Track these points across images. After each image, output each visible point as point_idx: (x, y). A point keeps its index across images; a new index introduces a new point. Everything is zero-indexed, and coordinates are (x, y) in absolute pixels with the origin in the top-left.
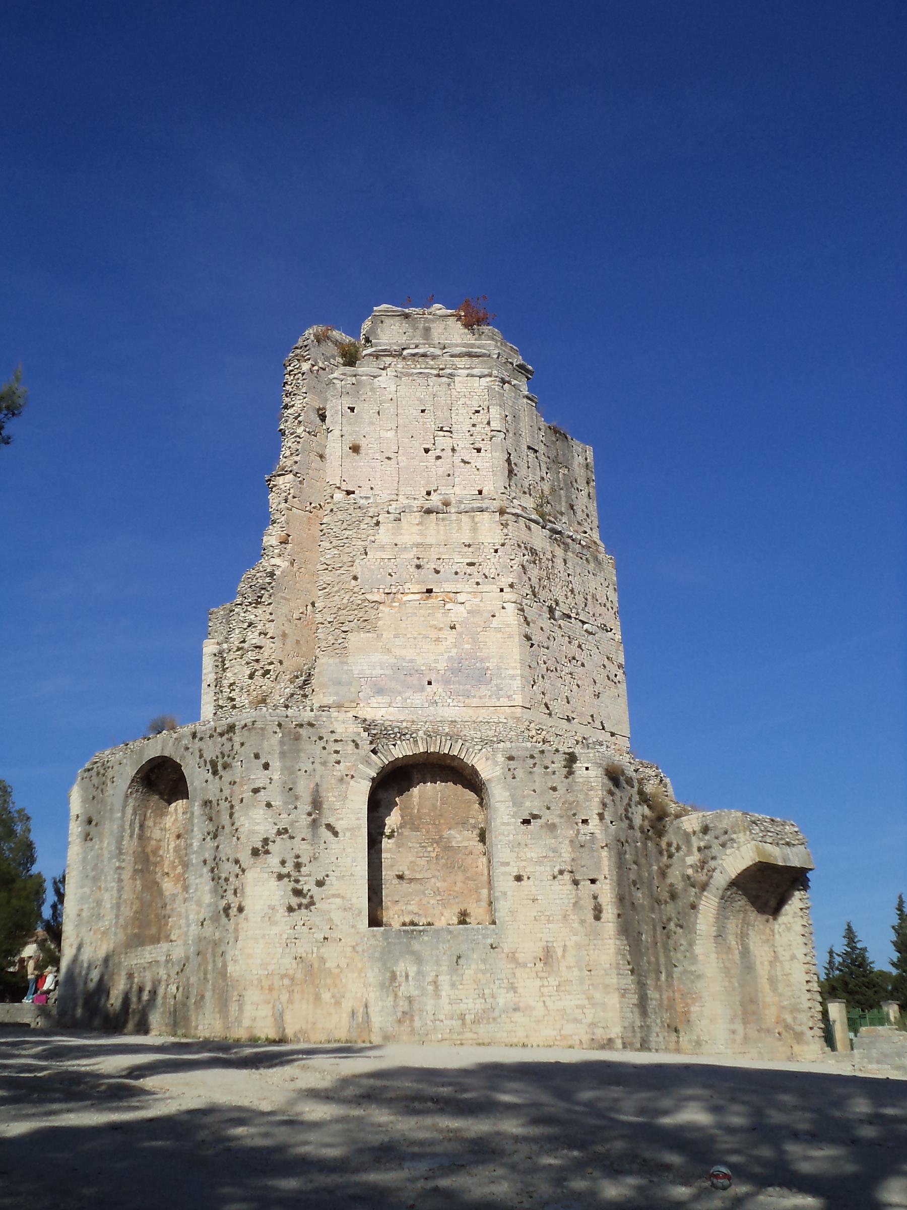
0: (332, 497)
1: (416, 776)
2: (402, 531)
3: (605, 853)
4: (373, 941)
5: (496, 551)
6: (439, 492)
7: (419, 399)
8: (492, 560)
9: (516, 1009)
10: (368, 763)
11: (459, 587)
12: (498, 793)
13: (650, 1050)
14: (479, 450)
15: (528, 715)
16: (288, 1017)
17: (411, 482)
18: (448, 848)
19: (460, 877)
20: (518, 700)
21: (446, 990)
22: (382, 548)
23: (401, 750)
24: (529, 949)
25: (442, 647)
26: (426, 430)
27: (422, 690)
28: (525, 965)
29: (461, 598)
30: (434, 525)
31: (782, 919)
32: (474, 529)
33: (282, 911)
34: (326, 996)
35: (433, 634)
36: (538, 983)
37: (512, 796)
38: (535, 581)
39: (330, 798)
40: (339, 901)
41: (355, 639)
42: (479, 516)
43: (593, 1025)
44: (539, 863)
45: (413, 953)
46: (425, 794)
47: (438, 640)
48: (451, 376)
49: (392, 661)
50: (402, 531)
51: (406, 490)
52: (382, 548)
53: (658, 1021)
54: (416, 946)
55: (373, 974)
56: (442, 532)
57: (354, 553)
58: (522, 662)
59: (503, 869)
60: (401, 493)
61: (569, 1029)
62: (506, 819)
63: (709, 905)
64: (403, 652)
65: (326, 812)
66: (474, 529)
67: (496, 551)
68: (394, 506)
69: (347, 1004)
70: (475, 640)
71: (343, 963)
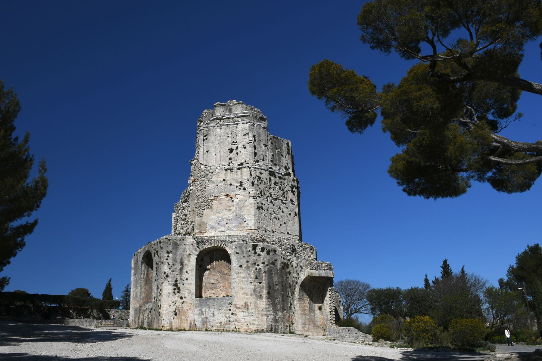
1: (215, 253)
7: (227, 133)
9: (236, 321)
10: (196, 251)
11: (236, 193)
12: (233, 258)
13: (278, 333)
14: (245, 148)
15: (256, 232)
16: (173, 324)
18: (223, 274)
19: (227, 282)
21: (216, 316)
22: (214, 182)
24: (240, 303)
25: (231, 212)
27: (225, 226)
28: (239, 308)
29: (237, 196)
32: (242, 174)
33: (172, 294)
34: (183, 318)
35: (228, 208)
36: (243, 313)
37: (237, 258)
38: (262, 189)
39: (185, 261)
40: (187, 291)
41: (206, 212)
43: (258, 325)
44: (244, 278)
47: (230, 210)
48: (237, 124)
51: (223, 163)
52: (214, 182)
53: (283, 324)
54: (208, 303)
55: (197, 311)
59: (234, 280)
61: (251, 326)
63: (297, 289)
65: (184, 265)
66: (242, 174)
69: (189, 320)
70: (240, 209)
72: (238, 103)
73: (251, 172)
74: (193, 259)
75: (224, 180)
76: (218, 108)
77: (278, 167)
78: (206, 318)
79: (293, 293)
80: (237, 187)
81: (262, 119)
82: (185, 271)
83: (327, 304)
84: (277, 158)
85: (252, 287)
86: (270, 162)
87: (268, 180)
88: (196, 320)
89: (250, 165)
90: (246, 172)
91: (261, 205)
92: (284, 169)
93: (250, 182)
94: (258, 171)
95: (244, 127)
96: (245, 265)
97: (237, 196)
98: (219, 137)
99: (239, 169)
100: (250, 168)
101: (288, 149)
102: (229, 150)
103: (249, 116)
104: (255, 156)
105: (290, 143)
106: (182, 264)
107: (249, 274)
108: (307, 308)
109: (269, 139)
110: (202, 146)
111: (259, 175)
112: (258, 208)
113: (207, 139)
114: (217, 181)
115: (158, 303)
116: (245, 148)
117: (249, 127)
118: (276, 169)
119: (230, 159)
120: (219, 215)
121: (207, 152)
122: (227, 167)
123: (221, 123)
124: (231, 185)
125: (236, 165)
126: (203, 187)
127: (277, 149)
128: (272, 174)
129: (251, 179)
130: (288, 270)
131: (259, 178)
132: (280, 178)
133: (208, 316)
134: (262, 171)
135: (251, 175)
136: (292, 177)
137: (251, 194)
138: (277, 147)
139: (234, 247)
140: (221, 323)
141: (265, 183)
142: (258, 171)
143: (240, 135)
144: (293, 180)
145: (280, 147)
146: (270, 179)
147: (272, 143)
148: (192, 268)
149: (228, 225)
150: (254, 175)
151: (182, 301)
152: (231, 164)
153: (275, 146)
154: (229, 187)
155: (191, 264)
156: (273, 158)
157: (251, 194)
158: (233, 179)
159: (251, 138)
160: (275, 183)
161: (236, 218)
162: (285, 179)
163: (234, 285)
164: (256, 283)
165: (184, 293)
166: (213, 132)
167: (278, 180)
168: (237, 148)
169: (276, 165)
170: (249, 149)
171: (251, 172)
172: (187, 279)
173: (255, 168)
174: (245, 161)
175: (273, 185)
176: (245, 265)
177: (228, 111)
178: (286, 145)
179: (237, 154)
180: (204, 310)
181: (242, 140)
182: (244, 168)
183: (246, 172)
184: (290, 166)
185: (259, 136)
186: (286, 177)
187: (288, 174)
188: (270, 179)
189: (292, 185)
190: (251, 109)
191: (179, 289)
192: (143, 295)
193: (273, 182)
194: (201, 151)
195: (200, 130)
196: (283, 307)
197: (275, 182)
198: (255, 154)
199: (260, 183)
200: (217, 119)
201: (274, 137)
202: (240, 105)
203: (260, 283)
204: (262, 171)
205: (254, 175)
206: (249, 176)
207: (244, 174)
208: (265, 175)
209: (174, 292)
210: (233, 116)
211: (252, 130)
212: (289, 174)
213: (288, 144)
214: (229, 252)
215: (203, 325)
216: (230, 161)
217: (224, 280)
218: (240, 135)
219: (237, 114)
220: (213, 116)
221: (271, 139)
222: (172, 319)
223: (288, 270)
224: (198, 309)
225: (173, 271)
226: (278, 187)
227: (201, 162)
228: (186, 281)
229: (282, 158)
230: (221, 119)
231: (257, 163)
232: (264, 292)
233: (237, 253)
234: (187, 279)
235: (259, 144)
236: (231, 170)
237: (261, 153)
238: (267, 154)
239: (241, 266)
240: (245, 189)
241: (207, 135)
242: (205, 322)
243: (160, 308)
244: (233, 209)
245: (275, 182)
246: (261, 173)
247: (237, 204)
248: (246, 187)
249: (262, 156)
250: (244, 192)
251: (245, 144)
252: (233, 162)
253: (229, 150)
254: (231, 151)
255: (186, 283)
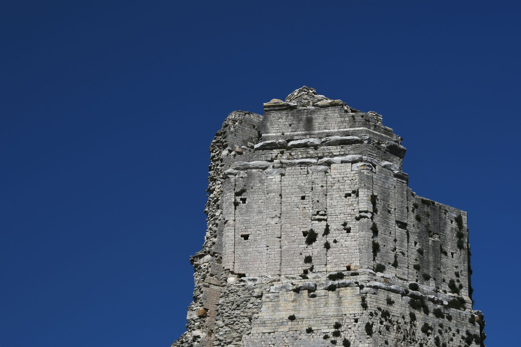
0: (226, 281)
2: (280, 308)
5: (356, 321)
6: (314, 271)
7: (300, 187)
8: (353, 329)
14: (348, 231)
17: (291, 263)
26: (305, 215)
30: (306, 301)
50: (280, 308)
51: (287, 270)
56: (312, 306)
57: (242, 329)
60: (282, 273)
67: (356, 321)
68: (274, 287)
72: (332, 105)
73: (363, 299)
75: (292, 318)
76: (274, 116)
77: (432, 285)
80: (326, 337)
81: (394, 150)
84: (431, 258)
86: (412, 270)
87: (408, 319)
89: (361, 279)
90: (350, 298)
92: (448, 289)
93: (361, 326)
94: (382, 296)
95: (345, 171)
98: (278, 198)
99: (332, 288)
100: (362, 287)
101: (460, 236)
102: (305, 234)
103: (361, 142)
104: (375, 255)
105: (464, 218)
109: (411, 207)
110: (231, 222)
111: (384, 306)
113: (244, 200)
114: (273, 321)
116: (348, 231)
117: (360, 173)
118: (427, 288)
119: (308, 260)
121: (246, 237)
122: (300, 283)
123: (284, 159)
124: (310, 331)
125: (323, 279)
126: (235, 334)
127: (430, 233)
128: (418, 303)
129: (365, 318)
131: (386, 314)
132: (438, 314)
134: (393, 296)
135: (364, 306)
136: (468, 311)
138: (432, 228)
141: (399, 328)
143: (336, 195)
144: (472, 321)
145: (440, 230)
146: (413, 317)
147: (418, 218)
150: (372, 308)
152: (310, 275)
153: (427, 226)
154: (304, 336)
156: (421, 259)
158: (316, 316)
159: (364, 203)
160: (426, 329)
162: (450, 318)
166: (261, 181)
167: (432, 320)
168: (327, 231)
169: (427, 278)
170: (360, 235)
171: (363, 299)
173: (376, 287)
174: (349, 268)
175: (419, 334)
177: (302, 124)
178: (454, 225)
179: (327, 246)
181: (340, 209)
182: (346, 285)
183: (350, 298)
184: (464, 280)
185: (385, 199)
186: (453, 311)
187: (459, 304)
188: (413, 317)
189: (468, 332)
190: (367, 122)
193: (419, 324)
194: (229, 235)
195: (226, 177)
197: (426, 325)
198: (376, 248)
199: (388, 328)
200: (272, 146)
201: (424, 202)
202: (337, 109)
204: (393, 296)
205: (372, 308)
206: (357, 309)
207: (346, 303)
208: (400, 307)
210: (317, 141)
211: (368, 181)
212: (459, 304)
213: (459, 220)
216: (308, 266)
218: (336, 195)
219: (328, 135)
220: (259, 138)
221: (416, 206)
227: (227, 264)
229: (444, 259)
230: (283, 147)
231: (379, 274)
235: (385, 222)
236: (311, 290)
237: (391, 245)
238: (404, 250)
241: (243, 191)
245: (426, 325)
246: (390, 302)
249: (392, 255)
251: (348, 219)
252: (316, 268)
253: (305, 234)
254: (311, 237)
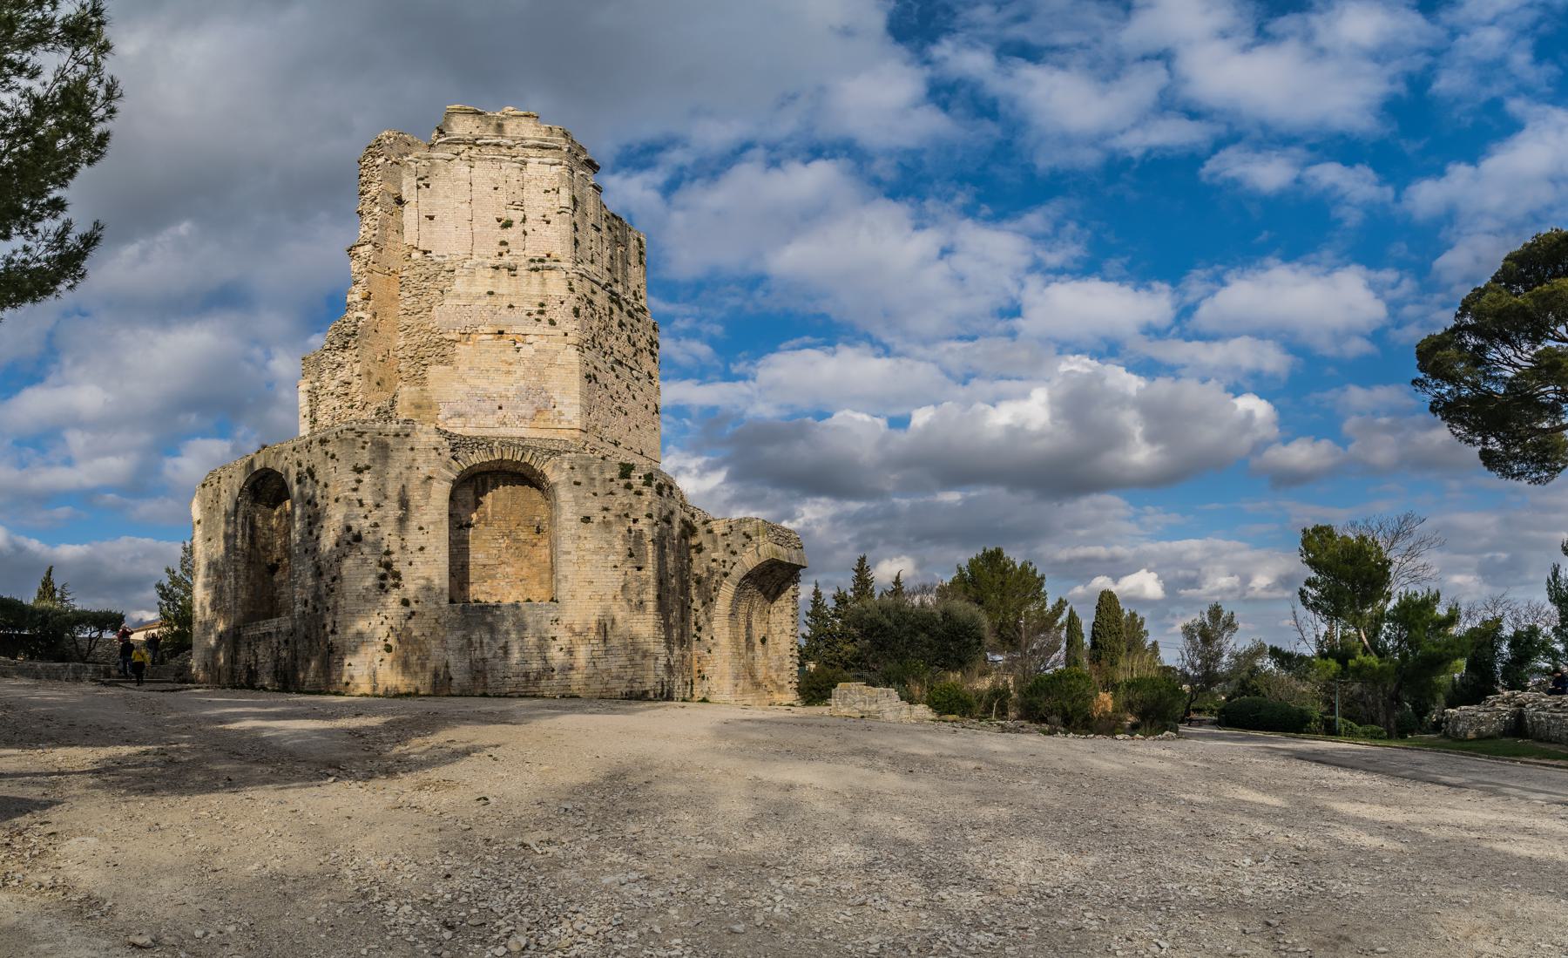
3: (650, 547)
4: (452, 615)
11: (527, 330)
12: (564, 495)
16: (380, 677)
18: (516, 540)
20: (577, 424)
23: (478, 458)
25: (511, 379)
29: (530, 339)
31: (777, 603)
32: (544, 283)
35: (505, 368)
39: (416, 497)
42: (547, 274)
43: (632, 680)
44: (595, 552)
45: (487, 624)
46: (496, 499)
49: (467, 389)
55: (454, 640)
58: (582, 394)
61: (614, 684)
62: (569, 516)
63: (726, 592)
64: (477, 382)
66: (544, 283)
69: (431, 665)
70: (540, 374)
71: (427, 632)
74: (440, 492)
78: (484, 660)
79: (708, 601)
82: (413, 524)
83: (783, 632)
85: (616, 578)
88: (452, 663)
91: (593, 371)
96: (598, 518)
97: (530, 339)
106: (404, 503)
107: (610, 543)
108: (743, 639)
112: (588, 376)
115: (322, 616)
118: (619, 289)
120: (477, 382)
128: (615, 298)
130: (694, 541)
132: (630, 315)
133: (489, 656)
134: (595, 287)
137: (572, 338)
139: (566, 466)
140: (526, 675)
142: (587, 283)
148: (436, 517)
149: (504, 411)
151: (407, 610)
154: (504, 312)
155: (434, 507)
157: (570, 339)
158: (517, 294)
160: (621, 324)
161: (527, 393)
163: (565, 569)
164: (628, 565)
165: (411, 587)
167: (626, 319)
172: (422, 549)
175: (616, 328)
176: (598, 518)
180: (475, 637)
191: (397, 575)
192: (243, 595)
193: (616, 319)
196: (682, 634)
203: (639, 569)
207: (550, 284)
208: (601, 299)
209: (382, 586)
214: (553, 476)
215: (474, 679)
217: (519, 555)
222: (377, 662)
223: (694, 541)
224: (459, 633)
225: (376, 525)
226: (625, 337)
228: (419, 554)
232: (650, 594)
233: (577, 483)
234: (422, 549)
239: (586, 520)
240: (552, 323)
242: (478, 671)
243: (333, 632)
244: (519, 371)
247: (531, 360)
248: (558, 320)
250: (551, 331)
255: (418, 559)
